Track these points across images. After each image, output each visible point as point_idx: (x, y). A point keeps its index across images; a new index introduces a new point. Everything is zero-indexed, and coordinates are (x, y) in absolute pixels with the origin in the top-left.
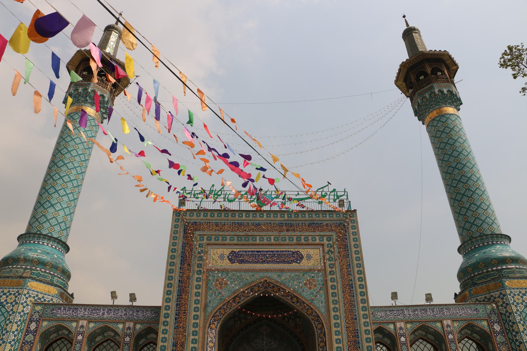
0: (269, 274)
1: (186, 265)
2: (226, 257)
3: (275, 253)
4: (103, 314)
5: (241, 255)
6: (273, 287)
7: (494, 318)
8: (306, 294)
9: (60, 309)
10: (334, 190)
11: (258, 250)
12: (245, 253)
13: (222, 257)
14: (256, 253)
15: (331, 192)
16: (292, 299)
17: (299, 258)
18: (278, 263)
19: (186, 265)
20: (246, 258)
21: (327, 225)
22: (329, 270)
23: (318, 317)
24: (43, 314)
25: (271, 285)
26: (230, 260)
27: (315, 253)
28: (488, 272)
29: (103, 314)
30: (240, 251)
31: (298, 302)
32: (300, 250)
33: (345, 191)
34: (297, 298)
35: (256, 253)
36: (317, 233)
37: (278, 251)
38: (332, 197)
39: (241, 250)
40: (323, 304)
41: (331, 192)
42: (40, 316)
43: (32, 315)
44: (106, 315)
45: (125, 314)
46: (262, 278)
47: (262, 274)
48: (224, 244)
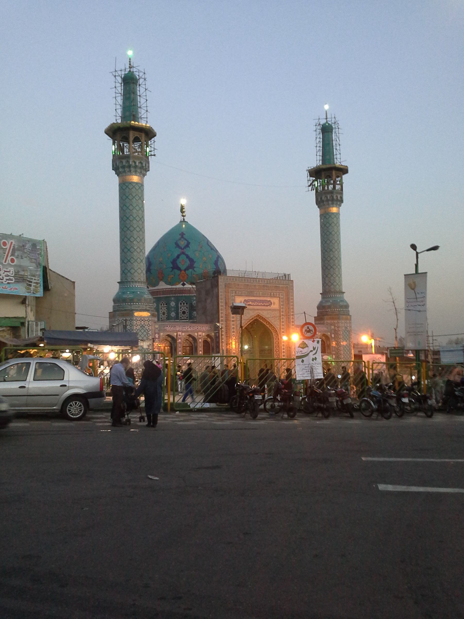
0: (260, 311)
1: (227, 306)
4: (188, 329)
6: (260, 317)
7: (333, 331)
8: (272, 321)
9: (167, 326)
16: (266, 323)
17: (270, 303)
19: (227, 306)
20: (250, 303)
21: (282, 287)
22: (281, 310)
23: (277, 331)
24: (159, 330)
25: (259, 316)
27: (275, 301)
28: (334, 311)
29: (188, 329)
30: (248, 300)
31: (268, 324)
32: (271, 300)
34: (269, 323)
35: (254, 301)
36: (278, 291)
37: (262, 300)
39: (249, 299)
40: (279, 326)
42: (158, 330)
43: (155, 330)
44: (189, 329)
45: (198, 329)
46: (257, 313)
47: (257, 311)
48: (242, 296)
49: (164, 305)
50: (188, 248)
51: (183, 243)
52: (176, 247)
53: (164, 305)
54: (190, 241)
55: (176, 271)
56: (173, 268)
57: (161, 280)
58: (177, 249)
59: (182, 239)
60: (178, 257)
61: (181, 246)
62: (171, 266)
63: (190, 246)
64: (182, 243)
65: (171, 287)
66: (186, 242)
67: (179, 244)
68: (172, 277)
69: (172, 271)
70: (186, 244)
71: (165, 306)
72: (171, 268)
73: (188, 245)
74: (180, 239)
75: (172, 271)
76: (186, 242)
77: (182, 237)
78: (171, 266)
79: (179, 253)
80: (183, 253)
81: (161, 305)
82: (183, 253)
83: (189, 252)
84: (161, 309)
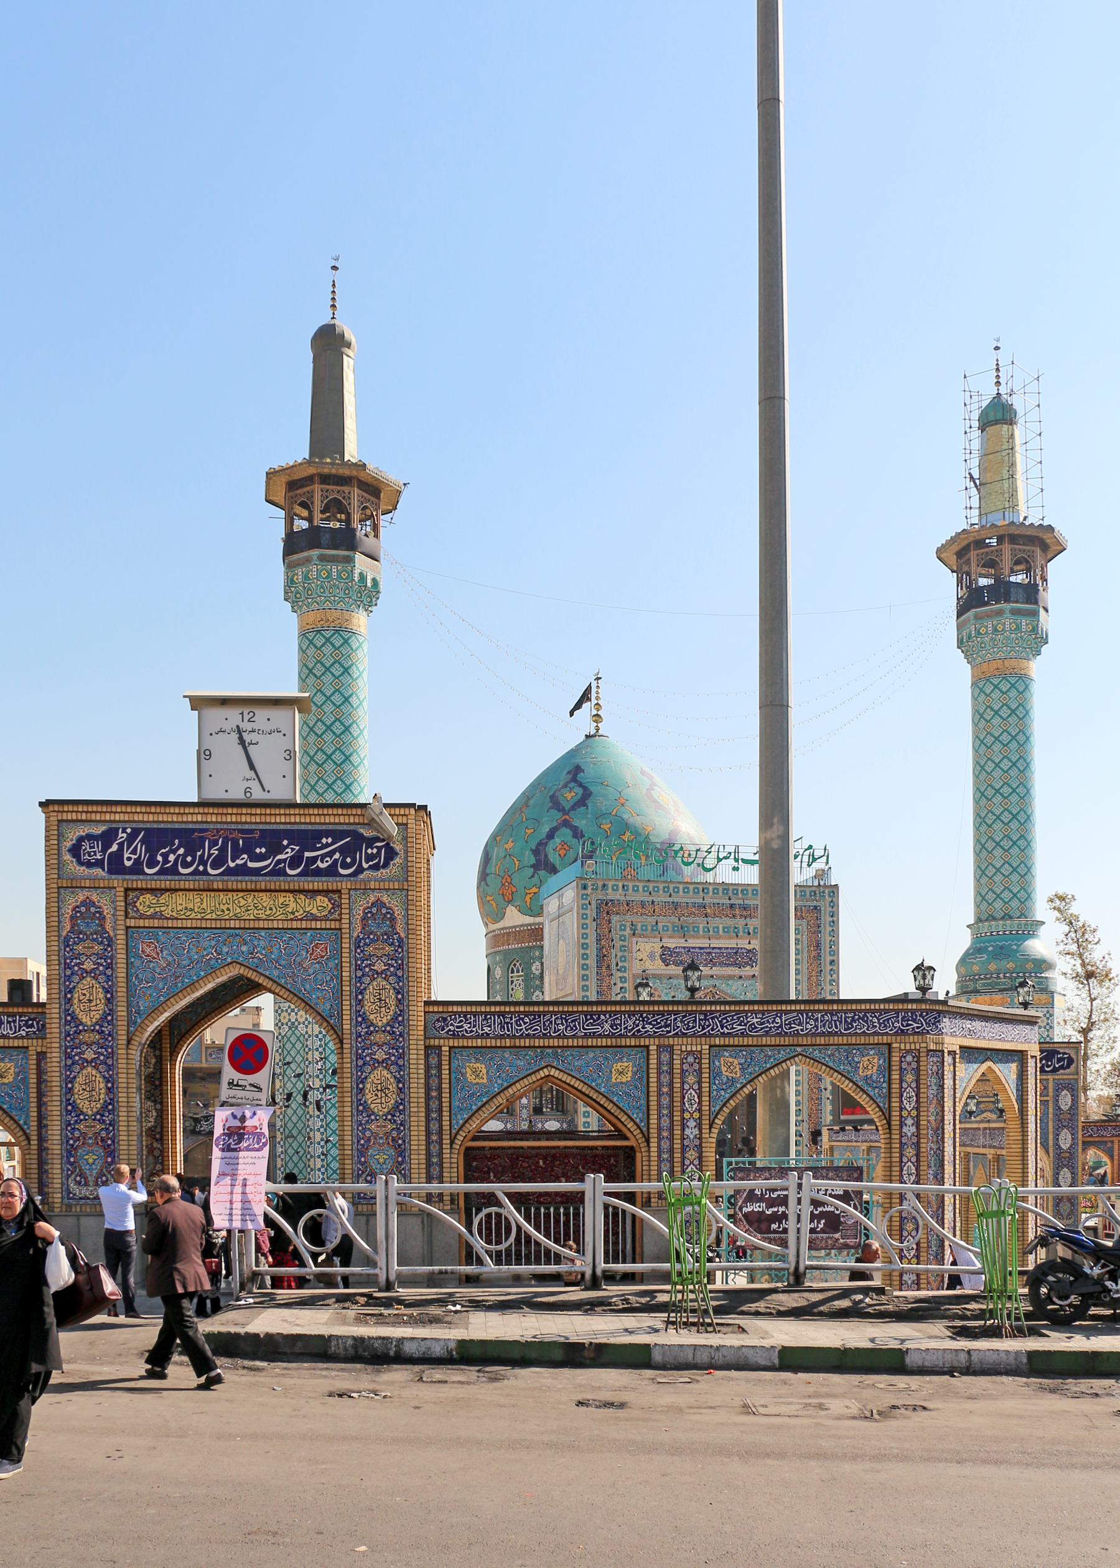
1: (604, 968)
2: (658, 957)
3: (723, 951)
5: (678, 953)
10: (810, 847)
11: (701, 945)
12: (683, 950)
13: (651, 956)
14: (697, 950)
15: (806, 850)
18: (728, 965)
26: (664, 961)
33: (825, 849)
35: (697, 950)
37: (727, 948)
38: (806, 859)
41: (806, 850)
49: (518, 972)
50: (583, 809)
51: (570, 796)
52: (550, 808)
53: (518, 972)
54: (592, 788)
55: (542, 873)
56: (536, 867)
57: (509, 902)
58: (554, 812)
59: (572, 785)
60: (551, 835)
61: (564, 803)
62: (533, 861)
63: (589, 805)
64: (569, 796)
65: (532, 922)
66: (580, 791)
67: (561, 800)
68: (535, 893)
69: (533, 876)
70: (579, 796)
71: (521, 973)
72: (532, 866)
73: (582, 802)
74: (565, 786)
75: (533, 876)
76: (580, 791)
77: (574, 779)
78: (533, 861)
79: (555, 824)
80: (566, 823)
81: (513, 972)
82: (566, 823)
83: (580, 821)
84: (512, 982)
